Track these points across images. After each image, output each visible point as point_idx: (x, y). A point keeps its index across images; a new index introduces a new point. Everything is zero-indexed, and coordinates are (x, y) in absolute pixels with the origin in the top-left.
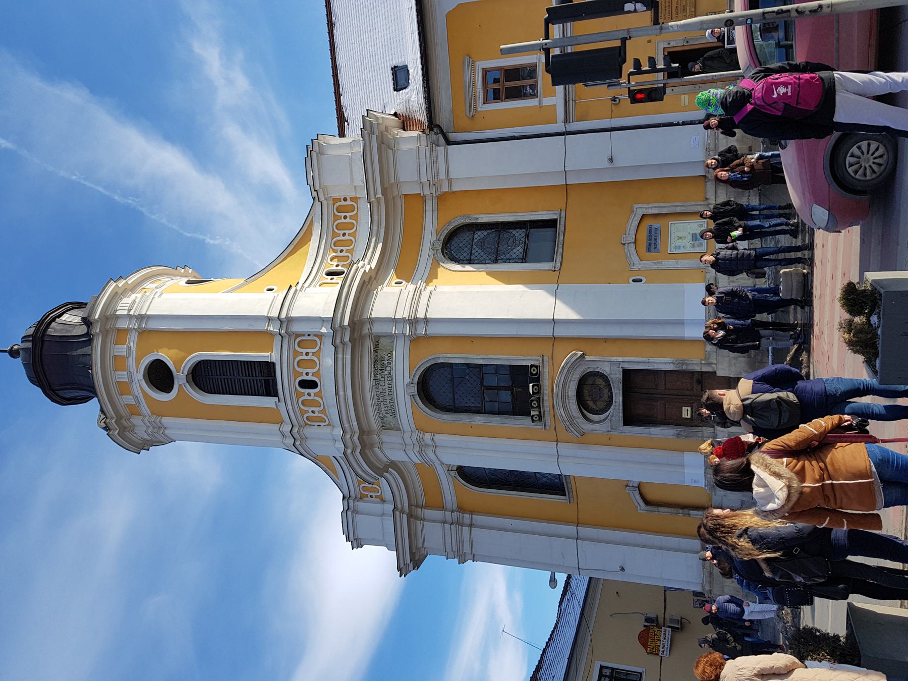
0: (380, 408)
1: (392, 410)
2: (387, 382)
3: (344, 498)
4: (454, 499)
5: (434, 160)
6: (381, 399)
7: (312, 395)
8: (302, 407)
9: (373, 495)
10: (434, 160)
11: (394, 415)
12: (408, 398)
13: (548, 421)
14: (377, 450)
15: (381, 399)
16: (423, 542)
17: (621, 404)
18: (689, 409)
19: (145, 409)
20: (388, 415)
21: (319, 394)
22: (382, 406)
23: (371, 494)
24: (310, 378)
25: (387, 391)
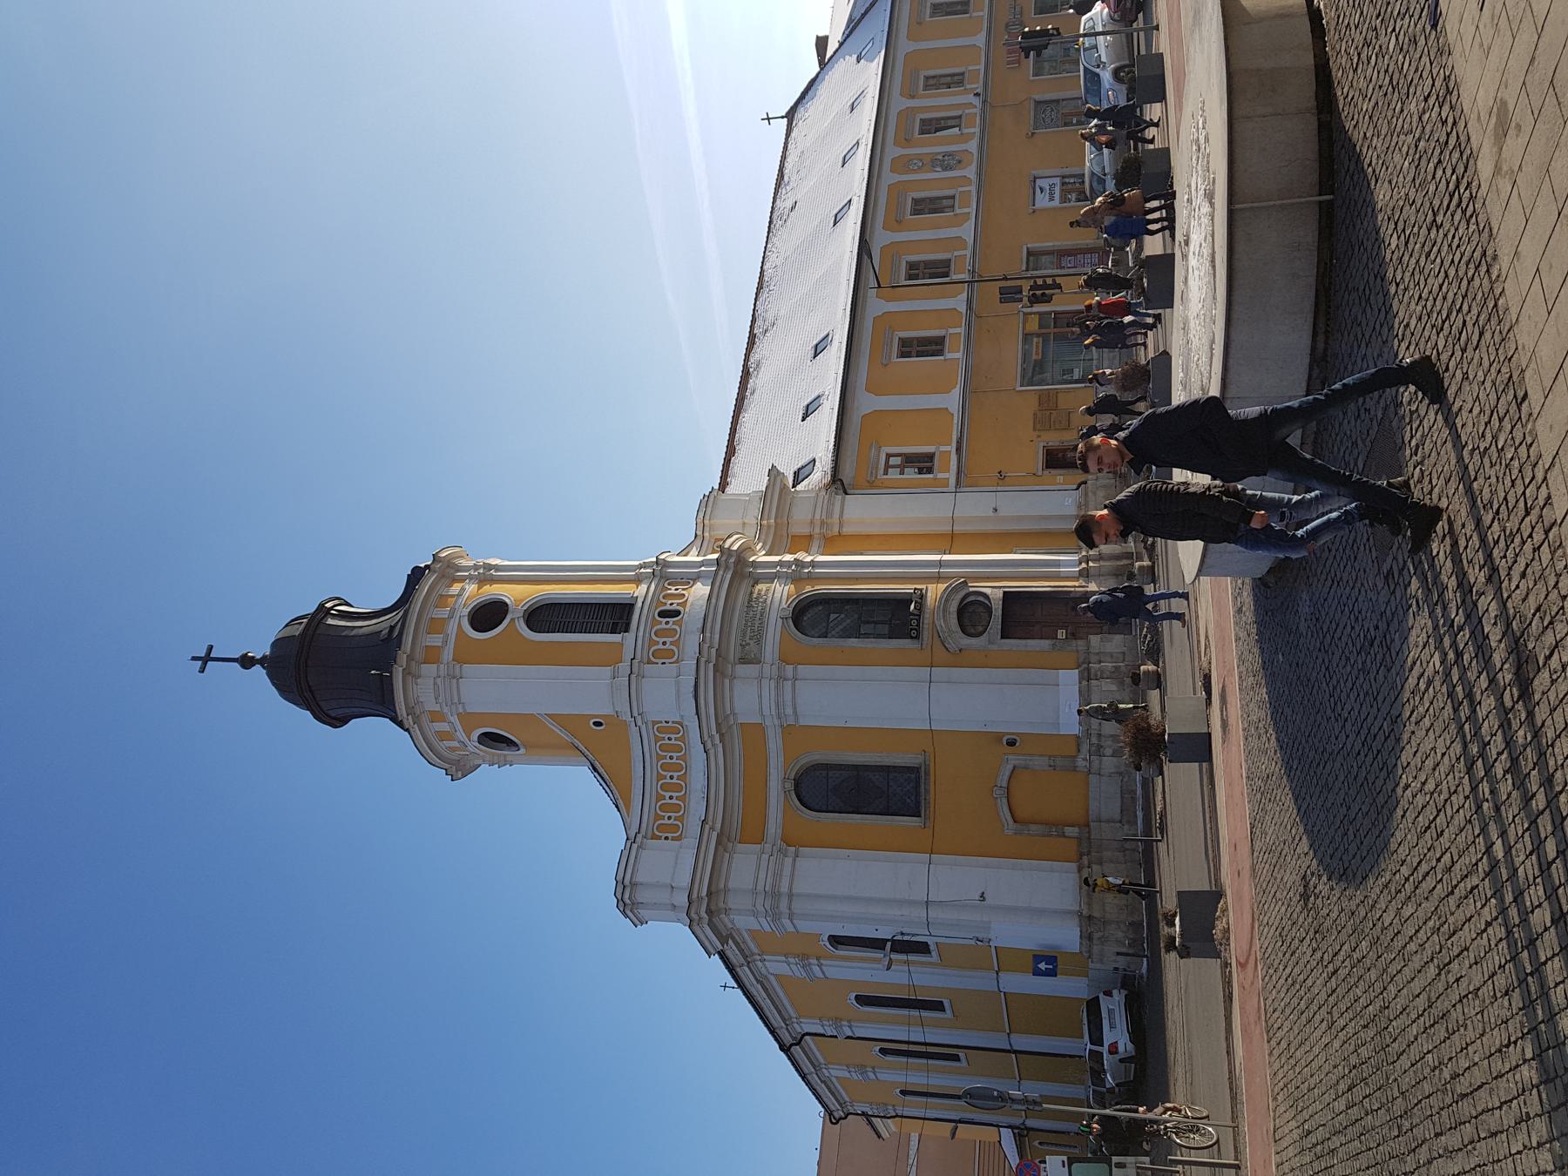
0: (744, 635)
1: (759, 638)
2: (760, 608)
3: (627, 839)
4: (780, 831)
5: (831, 503)
6: (749, 624)
7: (671, 623)
8: (654, 637)
9: (669, 835)
10: (831, 503)
11: (758, 642)
12: (780, 621)
13: (925, 639)
14: (727, 681)
15: (749, 624)
16: (727, 880)
17: (1000, 618)
18: (1064, 631)
19: (448, 654)
20: (752, 642)
21: (679, 624)
22: (749, 631)
23: (667, 835)
24: (675, 607)
25: (758, 616)
